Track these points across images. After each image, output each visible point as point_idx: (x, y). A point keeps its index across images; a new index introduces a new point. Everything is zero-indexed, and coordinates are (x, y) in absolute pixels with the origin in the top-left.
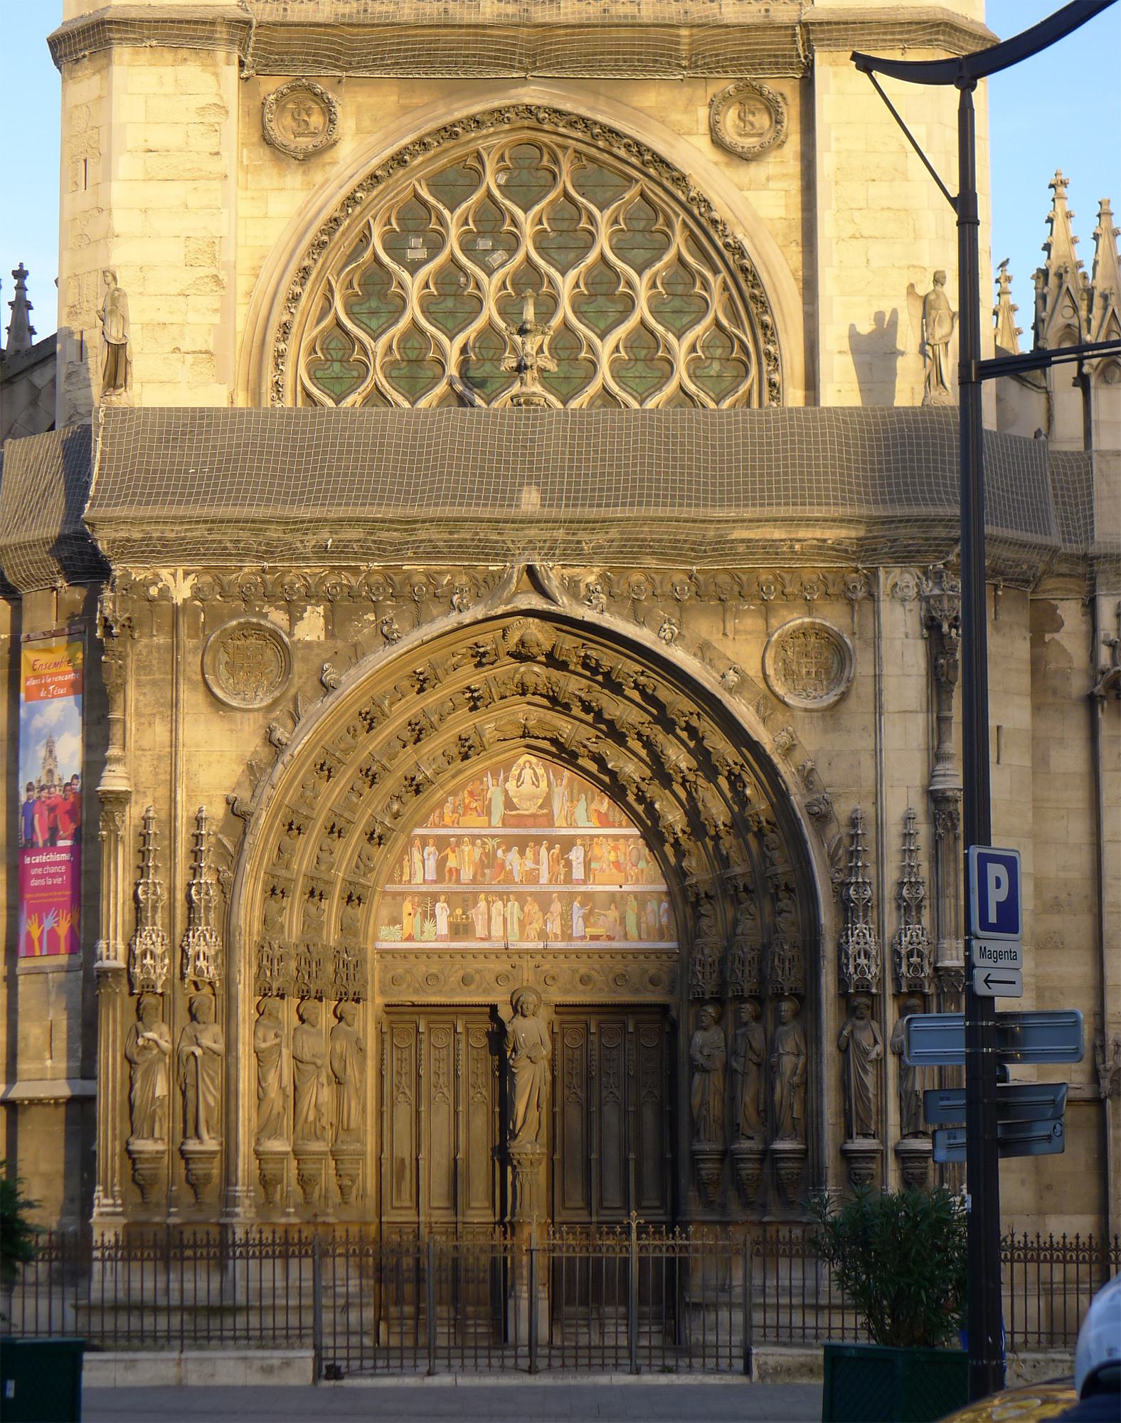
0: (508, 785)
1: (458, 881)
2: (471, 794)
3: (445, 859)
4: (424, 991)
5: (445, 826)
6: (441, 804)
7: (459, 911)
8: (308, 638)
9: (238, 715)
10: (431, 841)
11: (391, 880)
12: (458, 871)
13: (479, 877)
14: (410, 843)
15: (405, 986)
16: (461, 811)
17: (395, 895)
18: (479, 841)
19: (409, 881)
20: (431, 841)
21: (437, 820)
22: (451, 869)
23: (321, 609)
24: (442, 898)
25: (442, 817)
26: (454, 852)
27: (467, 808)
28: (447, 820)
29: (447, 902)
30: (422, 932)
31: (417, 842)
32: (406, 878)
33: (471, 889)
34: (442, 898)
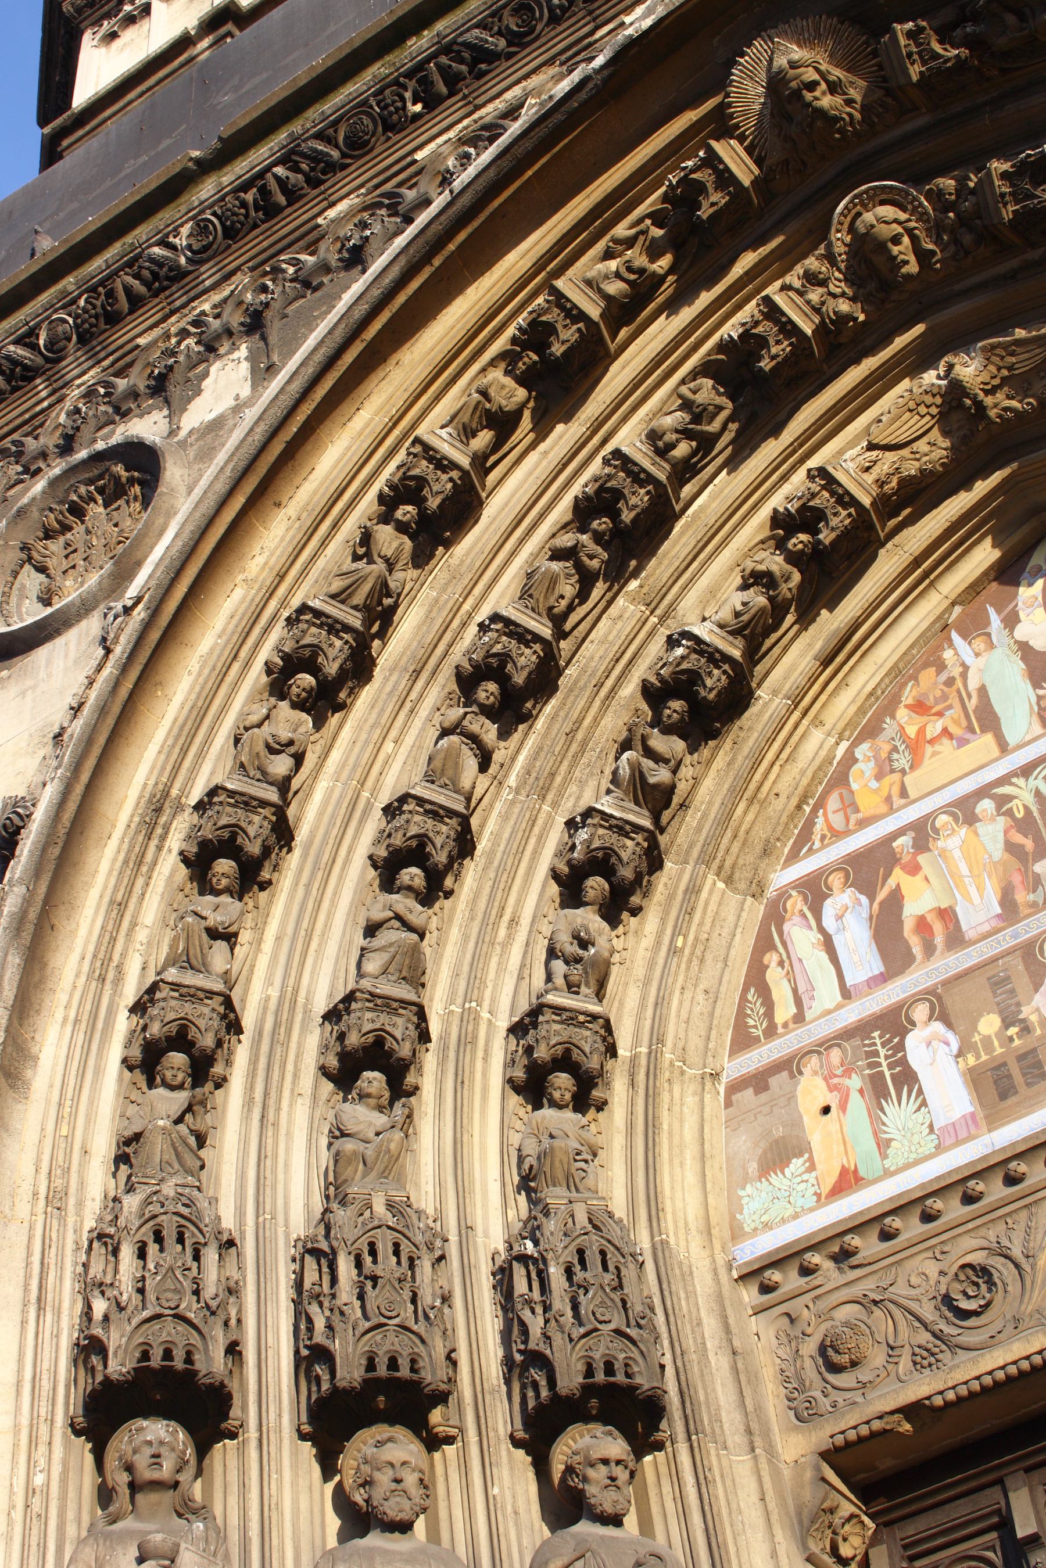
0: (1021, 632)
1: (956, 939)
2: (920, 707)
3: (896, 899)
4: (955, 1347)
5: (863, 824)
6: (841, 779)
7: (989, 1024)
8: (212, 416)
9: (41, 653)
10: (836, 880)
11: (743, 1040)
12: (947, 914)
13: (1021, 897)
14: (775, 915)
15: (877, 1357)
16: (902, 761)
17: (759, 1081)
18: (986, 805)
19: (799, 1018)
20: (836, 880)
21: (837, 821)
22: (922, 925)
23: (243, 351)
24: (920, 1013)
25: (850, 805)
26: (914, 869)
27: (916, 747)
28: (868, 803)
29: (942, 1015)
30: (883, 1145)
31: (796, 903)
32: (784, 1011)
33: (1007, 940)
34: (920, 1013)
